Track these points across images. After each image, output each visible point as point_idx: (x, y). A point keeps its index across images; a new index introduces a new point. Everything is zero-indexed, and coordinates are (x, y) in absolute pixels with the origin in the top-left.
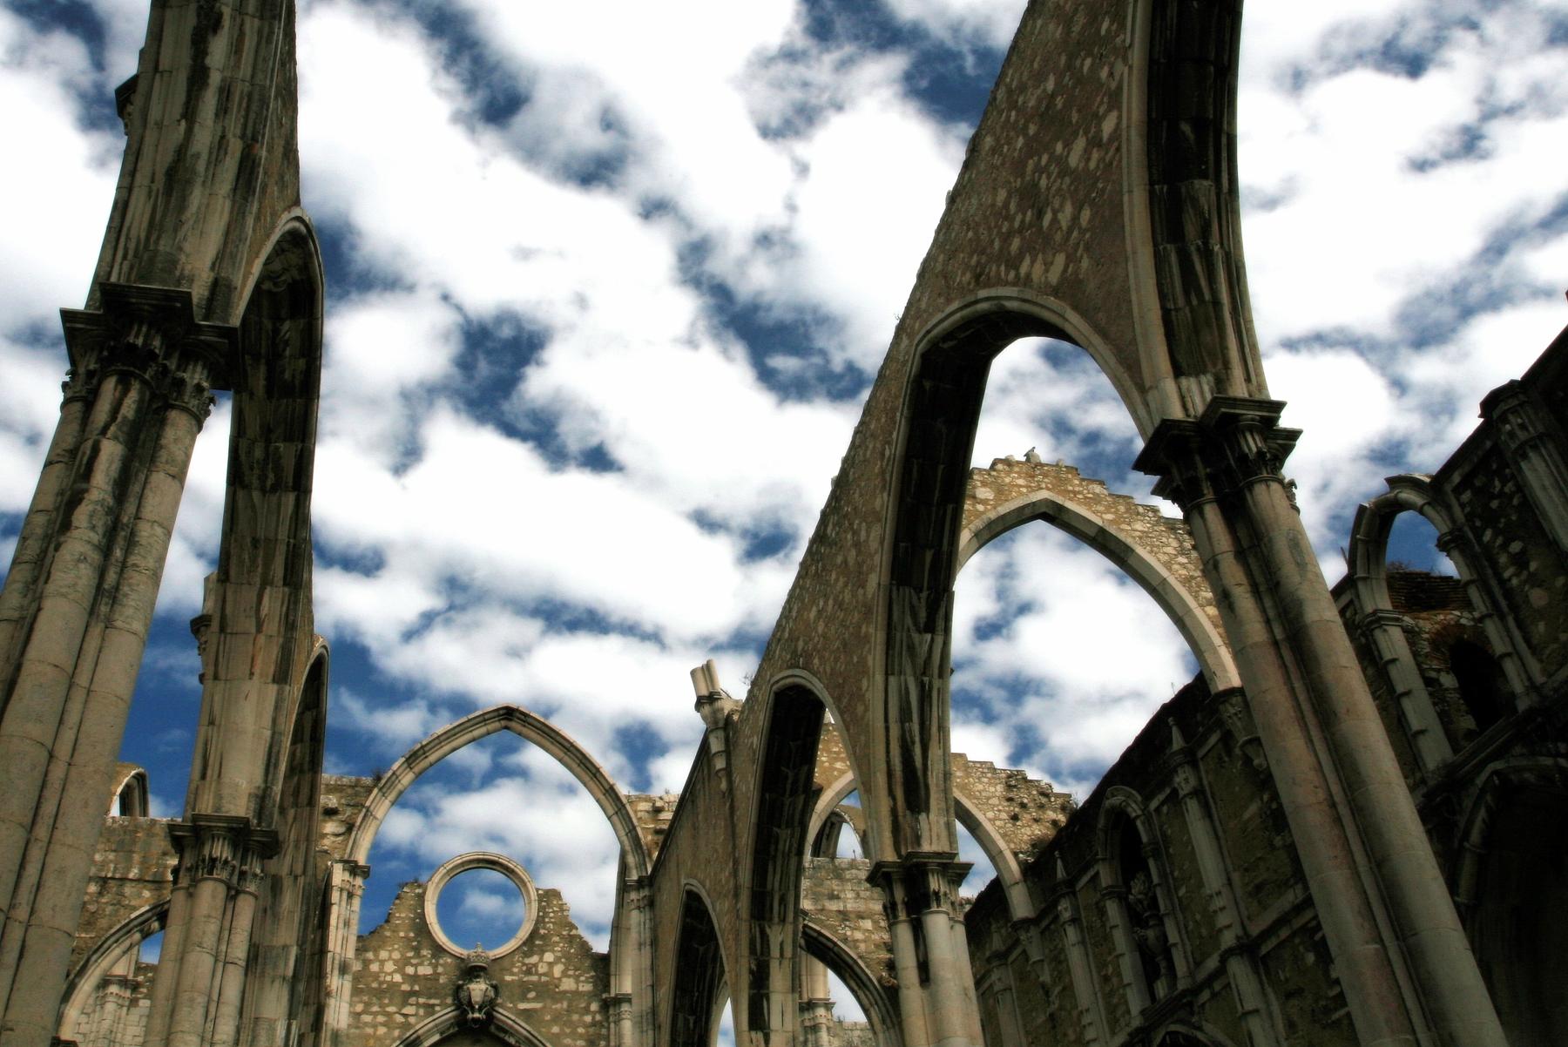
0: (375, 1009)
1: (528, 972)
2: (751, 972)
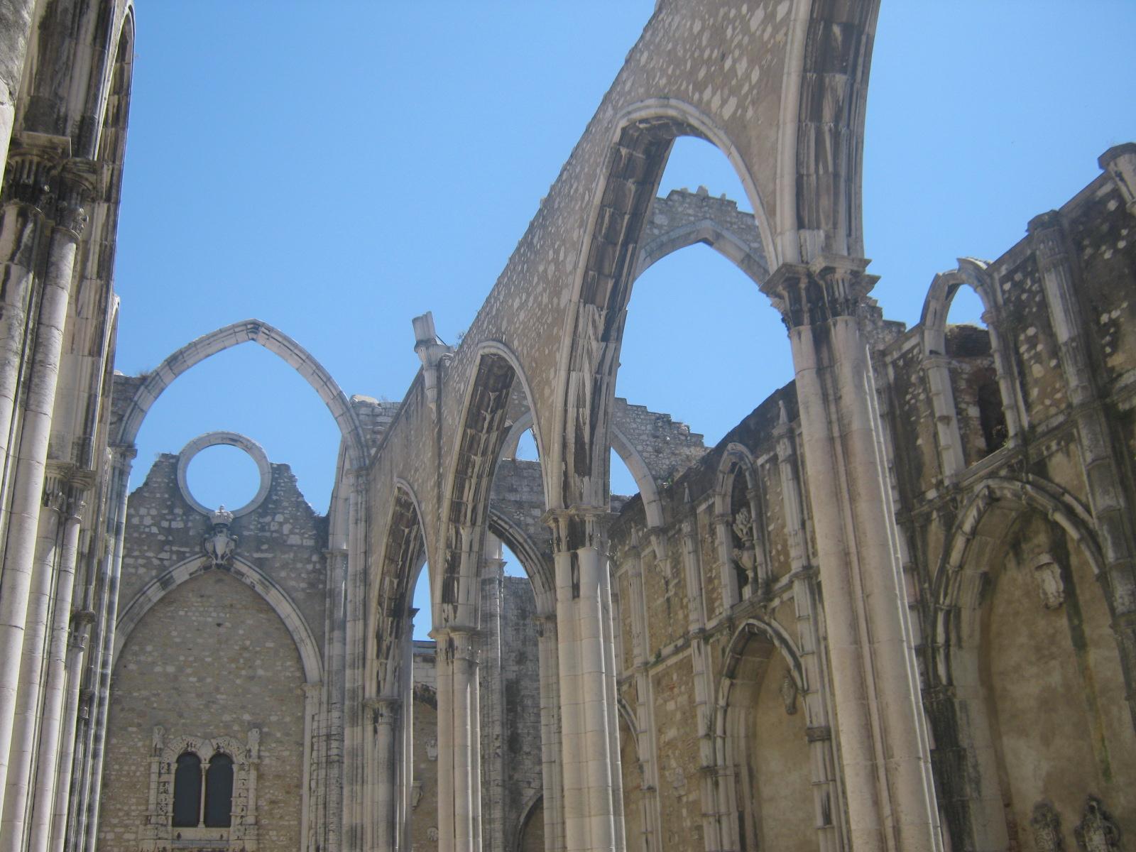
0: (136, 553)
1: (263, 529)
2: (447, 561)
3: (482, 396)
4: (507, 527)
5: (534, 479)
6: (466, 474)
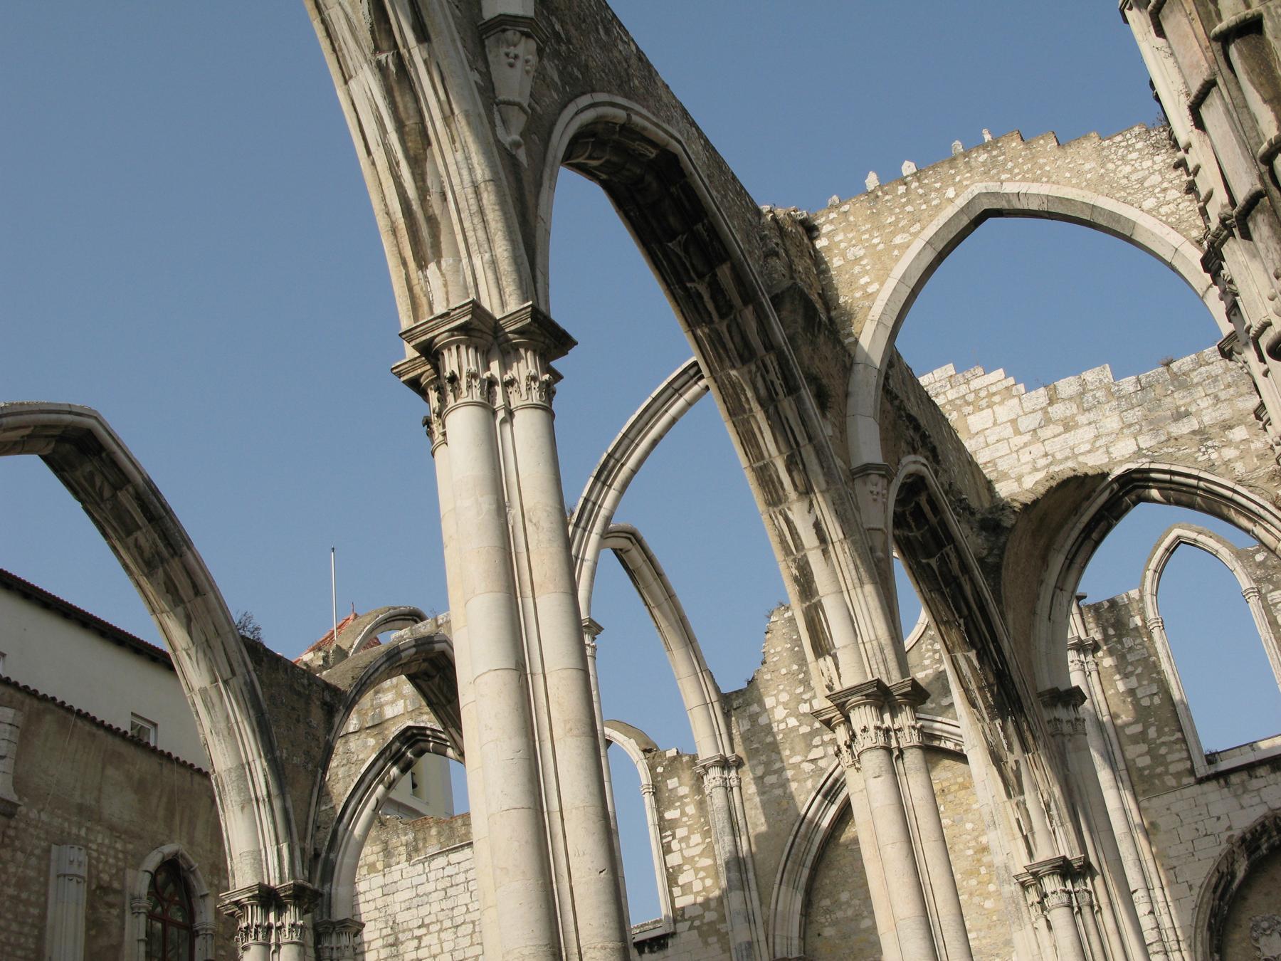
2: (796, 579)
3: (666, 255)
4: (1194, 482)
5: (1215, 379)
6: (745, 412)
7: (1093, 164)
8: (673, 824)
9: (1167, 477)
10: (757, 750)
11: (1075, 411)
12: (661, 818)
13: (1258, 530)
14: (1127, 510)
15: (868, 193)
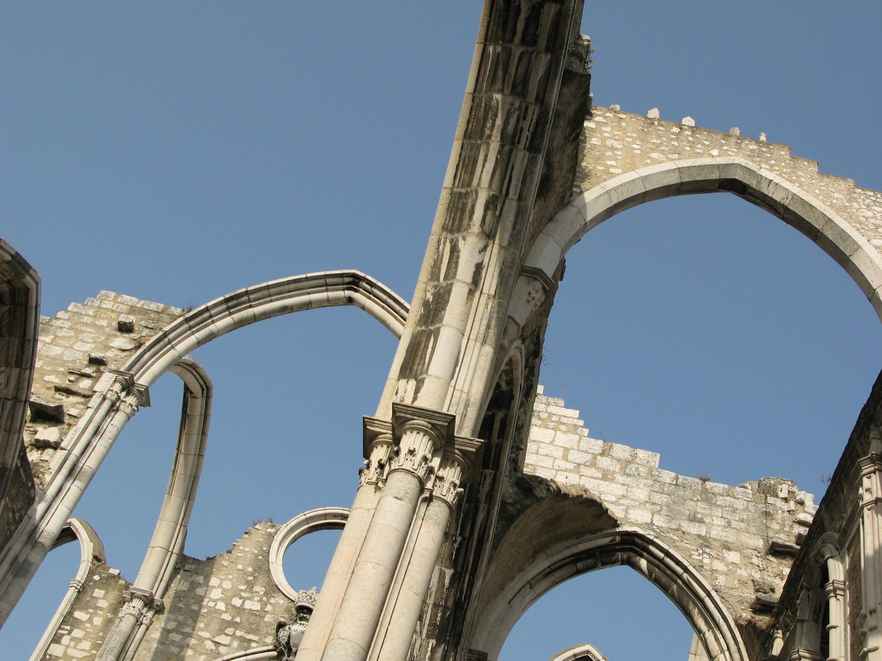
2: (426, 304)
4: (679, 570)
5: (735, 511)
7: (841, 197)
8: (76, 623)
9: (661, 555)
10: (180, 609)
11: (618, 468)
12: (70, 613)
13: (709, 636)
14: (613, 563)
15: (646, 118)
